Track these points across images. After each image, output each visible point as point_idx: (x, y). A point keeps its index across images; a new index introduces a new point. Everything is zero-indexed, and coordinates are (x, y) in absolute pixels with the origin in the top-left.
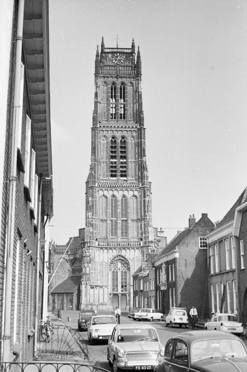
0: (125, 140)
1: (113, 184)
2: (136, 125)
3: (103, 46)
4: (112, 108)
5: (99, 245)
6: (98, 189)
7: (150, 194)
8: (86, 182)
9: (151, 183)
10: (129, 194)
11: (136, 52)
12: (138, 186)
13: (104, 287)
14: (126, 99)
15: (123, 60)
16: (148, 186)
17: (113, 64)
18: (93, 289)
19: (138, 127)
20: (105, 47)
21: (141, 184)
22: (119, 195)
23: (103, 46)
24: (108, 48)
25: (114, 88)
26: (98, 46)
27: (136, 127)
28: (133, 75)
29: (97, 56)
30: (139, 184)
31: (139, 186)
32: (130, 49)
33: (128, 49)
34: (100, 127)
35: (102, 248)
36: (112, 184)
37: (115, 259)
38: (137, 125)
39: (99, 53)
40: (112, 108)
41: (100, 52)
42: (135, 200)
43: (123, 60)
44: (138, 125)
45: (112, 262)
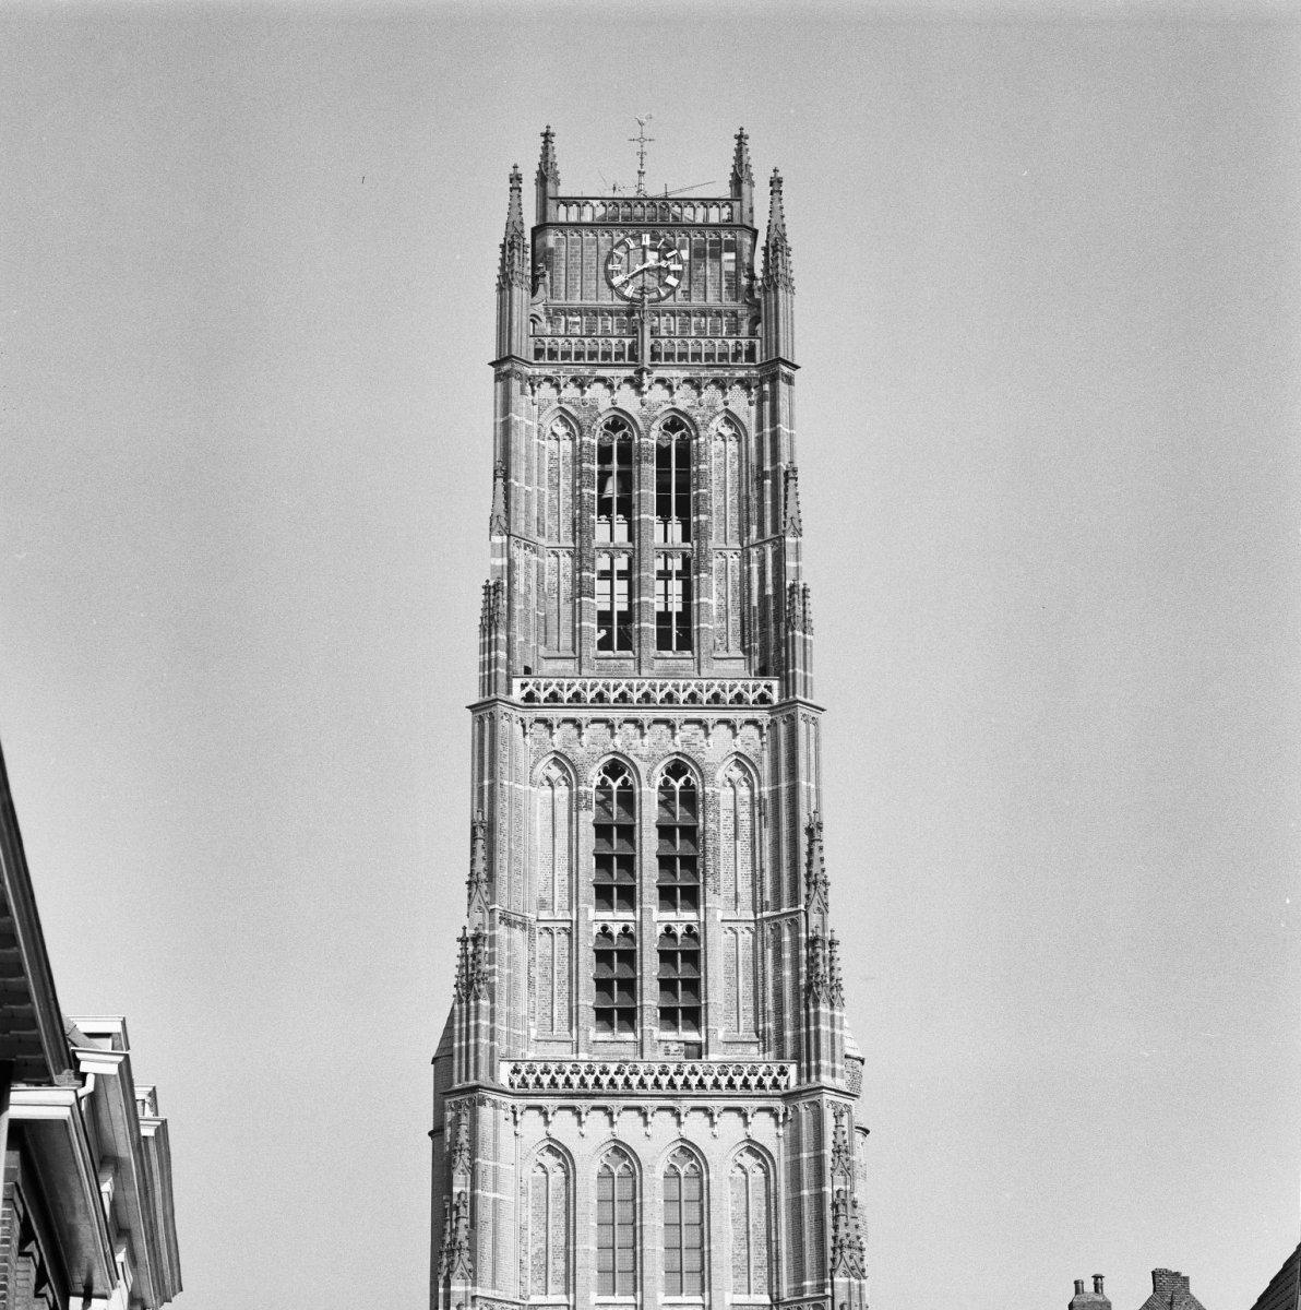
0: (688, 780)
2: (761, 690)
3: (544, 177)
4: (606, 575)
6: (510, 1101)
7: (858, 1136)
8: (433, 1053)
9: (862, 1061)
10: (721, 1139)
12: (775, 1085)
14: (695, 519)
15: (677, 274)
16: (840, 1084)
19: (775, 697)
21: (792, 1070)
22: (654, 1140)
23: (544, 177)
25: (618, 448)
26: (516, 179)
27: (763, 699)
28: (742, 367)
29: (509, 246)
30: (783, 1072)
31: (782, 1081)
34: (530, 697)
36: (605, 1071)
38: (769, 688)
39: (520, 234)
40: (606, 575)
41: (530, 221)
42: (759, 1171)
43: (677, 274)
44: (775, 684)
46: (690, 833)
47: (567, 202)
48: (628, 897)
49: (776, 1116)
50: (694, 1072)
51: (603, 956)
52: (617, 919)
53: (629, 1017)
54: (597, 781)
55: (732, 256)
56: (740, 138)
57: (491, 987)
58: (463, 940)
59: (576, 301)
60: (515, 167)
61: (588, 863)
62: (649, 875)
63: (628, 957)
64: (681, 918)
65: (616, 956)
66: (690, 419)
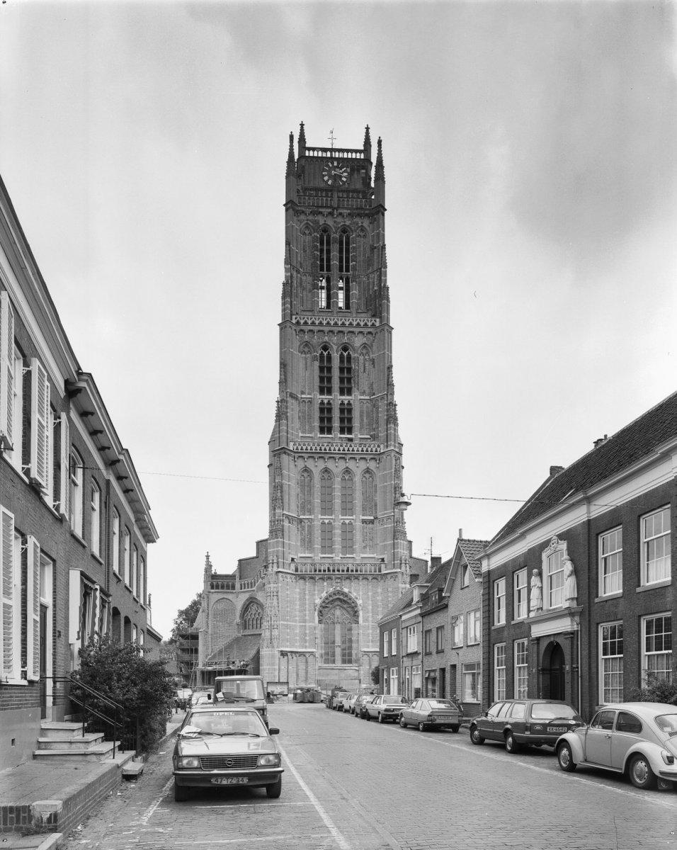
1: (326, 444)
5: (297, 570)
8: (268, 440)
11: (374, 160)
13: (307, 655)
17: (322, 185)
18: (286, 657)
20: (307, 145)
23: (302, 139)
24: (314, 149)
27: (373, 325)
30: (379, 446)
32: (360, 151)
33: (356, 151)
35: (303, 577)
37: (331, 599)
41: (296, 157)
44: (378, 320)
45: (324, 605)
46: (349, 370)
47: (309, 149)
48: (329, 392)
49: (376, 460)
50: (351, 446)
51: (322, 410)
52: (326, 398)
53: (329, 431)
54: (320, 352)
55: (364, 171)
56: (367, 129)
57: (287, 417)
58: (278, 402)
59: (312, 185)
60: (291, 132)
61: (317, 380)
62: (336, 384)
63: (330, 410)
64: (346, 398)
65: (325, 410)
66: (350, 228)
